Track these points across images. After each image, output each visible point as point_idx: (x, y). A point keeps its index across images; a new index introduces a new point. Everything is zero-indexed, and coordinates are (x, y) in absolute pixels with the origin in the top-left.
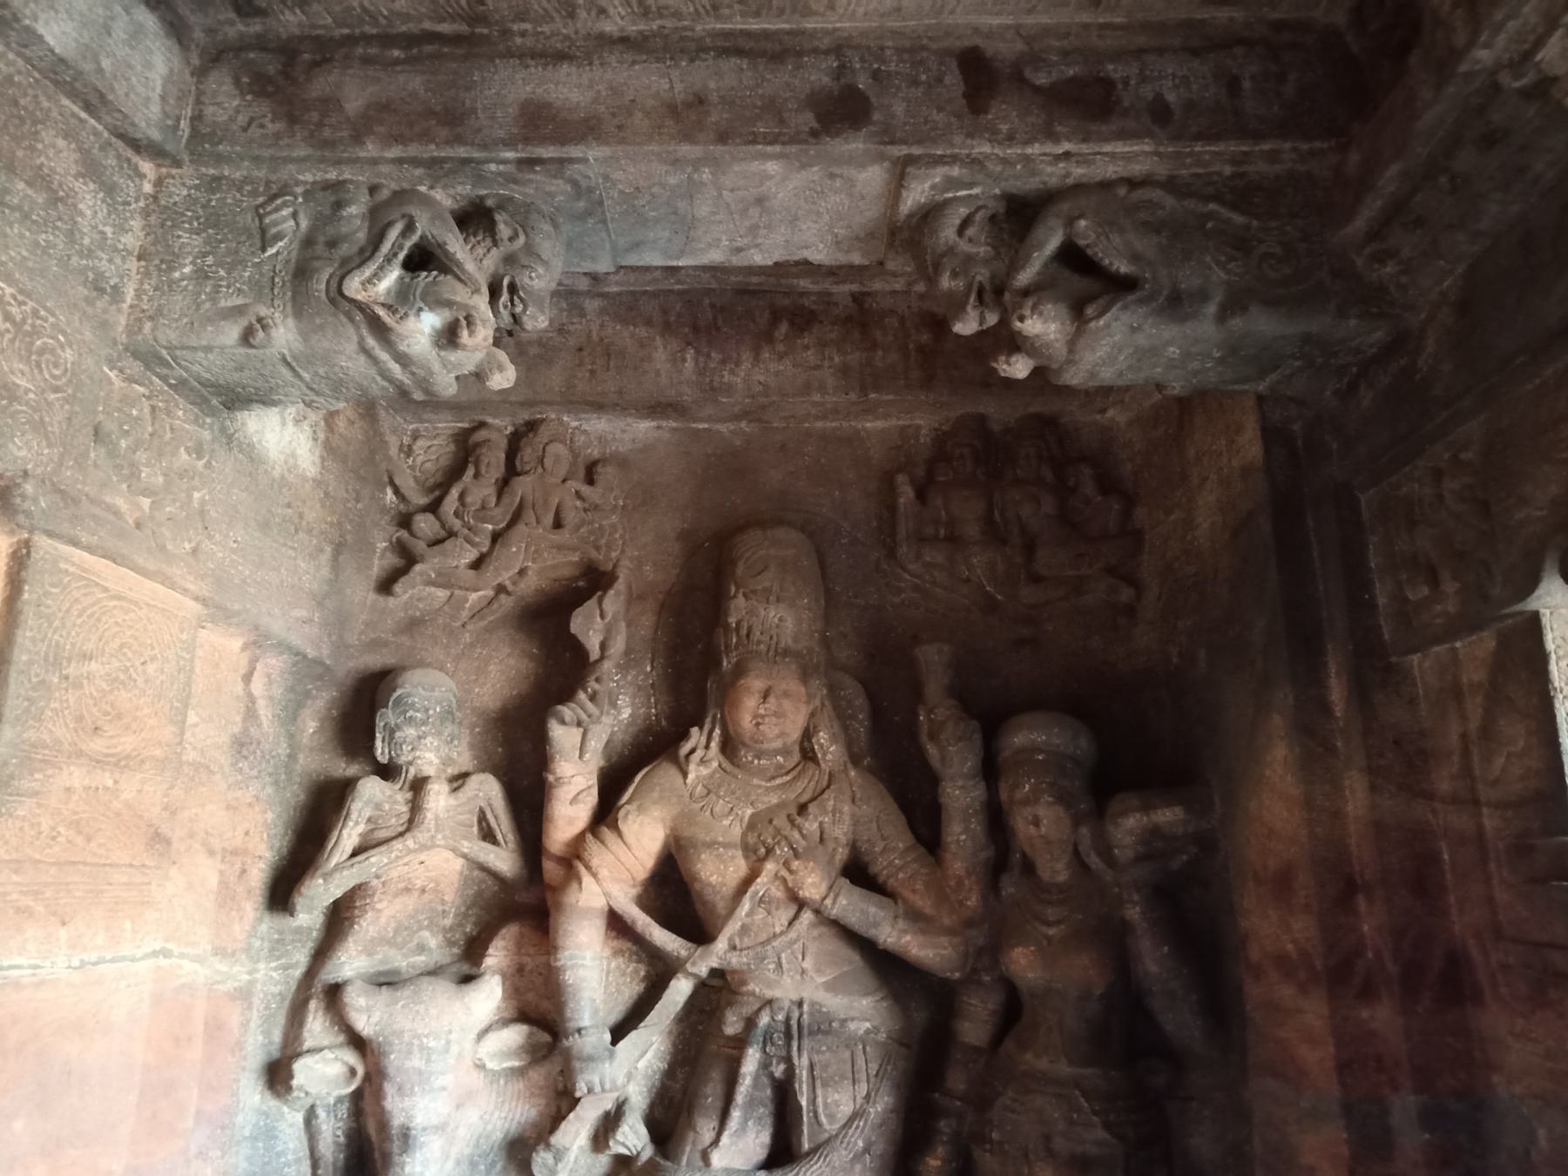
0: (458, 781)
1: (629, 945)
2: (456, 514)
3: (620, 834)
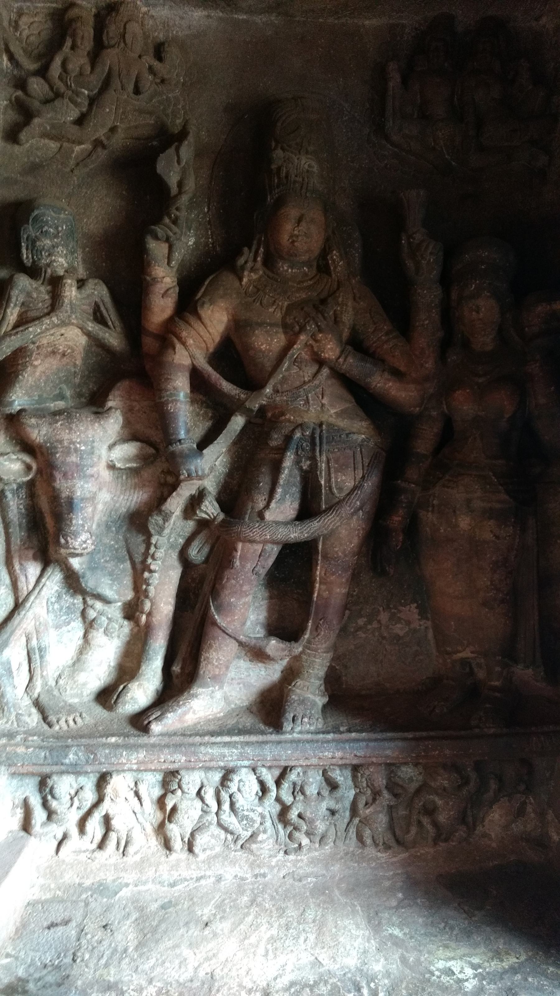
0: (81, 284)
1: (201, 397)
2: (60, 78)
3: (200, 318)
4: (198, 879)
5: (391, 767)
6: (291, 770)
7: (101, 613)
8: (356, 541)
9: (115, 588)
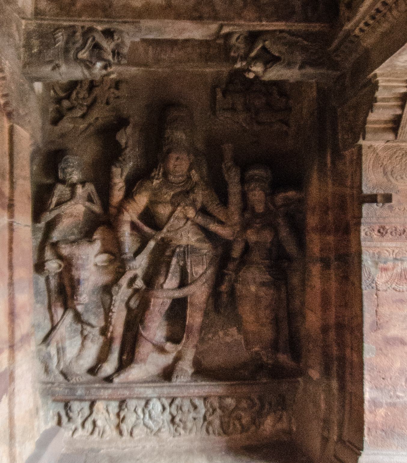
4: (135, 447)
5: (221, 398)
6: (176, 399)
7: (90, 332)
8: (204, 297)
9: (96, 321)
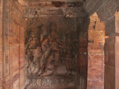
0: (35, 38)
